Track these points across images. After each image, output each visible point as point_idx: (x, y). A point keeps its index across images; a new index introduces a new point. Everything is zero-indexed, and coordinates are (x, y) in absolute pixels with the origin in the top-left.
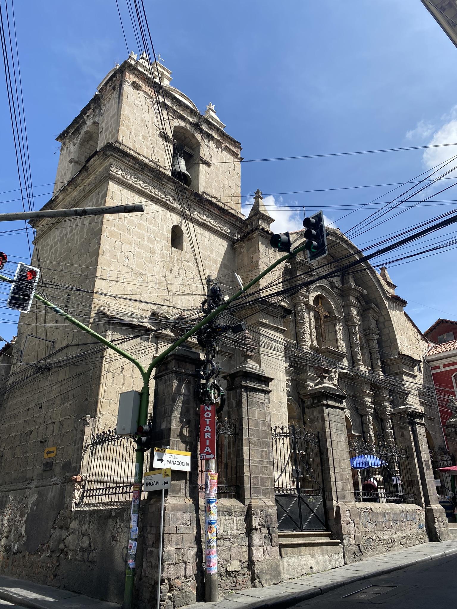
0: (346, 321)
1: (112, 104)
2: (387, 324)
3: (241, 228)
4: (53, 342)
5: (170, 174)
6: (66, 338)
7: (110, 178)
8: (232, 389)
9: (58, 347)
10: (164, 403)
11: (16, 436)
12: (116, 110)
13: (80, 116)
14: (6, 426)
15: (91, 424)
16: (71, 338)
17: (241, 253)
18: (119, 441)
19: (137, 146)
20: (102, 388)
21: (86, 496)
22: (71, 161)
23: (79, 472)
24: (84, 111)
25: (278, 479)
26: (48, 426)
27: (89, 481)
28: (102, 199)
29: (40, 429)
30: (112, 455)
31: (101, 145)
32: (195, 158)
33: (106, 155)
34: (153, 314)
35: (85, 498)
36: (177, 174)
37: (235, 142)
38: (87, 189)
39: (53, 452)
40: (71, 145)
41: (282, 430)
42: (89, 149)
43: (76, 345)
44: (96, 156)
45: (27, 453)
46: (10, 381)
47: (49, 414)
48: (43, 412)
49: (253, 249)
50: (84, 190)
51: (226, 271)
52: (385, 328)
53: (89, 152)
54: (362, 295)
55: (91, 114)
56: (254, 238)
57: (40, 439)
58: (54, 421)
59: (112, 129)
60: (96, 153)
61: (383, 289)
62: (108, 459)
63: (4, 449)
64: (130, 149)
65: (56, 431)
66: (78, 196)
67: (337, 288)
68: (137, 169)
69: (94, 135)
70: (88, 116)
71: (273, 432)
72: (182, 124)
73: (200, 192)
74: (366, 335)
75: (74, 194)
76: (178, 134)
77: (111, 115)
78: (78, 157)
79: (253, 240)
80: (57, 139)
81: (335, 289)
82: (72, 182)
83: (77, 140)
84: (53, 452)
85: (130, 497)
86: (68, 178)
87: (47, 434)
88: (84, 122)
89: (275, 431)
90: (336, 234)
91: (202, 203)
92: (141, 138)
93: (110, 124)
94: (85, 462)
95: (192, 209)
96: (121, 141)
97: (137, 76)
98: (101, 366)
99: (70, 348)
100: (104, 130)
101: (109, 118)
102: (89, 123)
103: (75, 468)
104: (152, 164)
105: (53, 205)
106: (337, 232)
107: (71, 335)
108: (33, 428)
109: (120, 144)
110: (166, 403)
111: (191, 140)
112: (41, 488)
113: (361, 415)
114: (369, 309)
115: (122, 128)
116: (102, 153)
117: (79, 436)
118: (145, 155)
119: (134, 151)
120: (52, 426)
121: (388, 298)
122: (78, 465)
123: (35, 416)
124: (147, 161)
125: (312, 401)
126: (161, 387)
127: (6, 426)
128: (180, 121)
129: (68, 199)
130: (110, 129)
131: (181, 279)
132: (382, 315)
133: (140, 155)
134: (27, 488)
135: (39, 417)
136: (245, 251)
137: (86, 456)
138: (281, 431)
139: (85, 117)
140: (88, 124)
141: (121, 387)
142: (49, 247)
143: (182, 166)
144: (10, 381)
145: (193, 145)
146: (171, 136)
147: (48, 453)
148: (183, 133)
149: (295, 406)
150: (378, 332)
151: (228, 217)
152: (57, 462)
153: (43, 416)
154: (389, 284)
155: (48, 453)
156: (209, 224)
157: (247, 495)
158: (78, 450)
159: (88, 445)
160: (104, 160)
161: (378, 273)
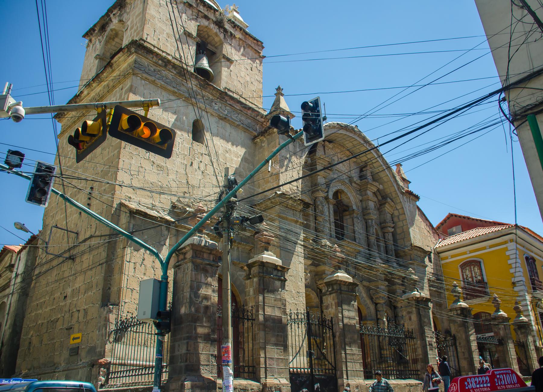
0: (364, 215)
1: (138, 4)
2: (401, 217)
3: (262, 123)
5: (192, 70)
6: (90, 229)
8: (250, 278)
9: (81, 238)
10: (183, 291)
11: (43, 323)
12: (141, 10)
13: (107, 15)
14: (33, 314)
15: (114, 311)
16: (94, 230)
17: (261, 147)
18: (141, 327)
19: (161, 44)
20: (125, 278)
21: (111, 378)
23: (103, 356)
24: (110, 11)
25: (292, 360)
27: (113, 364)
28: (125, 94)
29: (66, 317)
30: (134, 340)
31: (126, 42)
32: (218, 55)
33: (130, 52)
34: (174, 207)
35: (110, 380)
36: (201, 71)
37: (257, 41)
38: (111, 84)
39: (78, 338)
40: (98, 42)
41: (298, 316)
42: (114, 46)
43: (98, 236)
44: (121, 53)
45: (53, 339)
46: (37, 272)
47: (75, 302)
48: (69, 301)
49: (273, 143)
50: (108, 85)
51: (247, 165)
52: (400, 221)
53: (115, 48)
54: (378, 190)
55: (117, 13)
57: (65, 326)
58: (78, 309)
59: (137, 27)
60: (121, 50)
61: (398, 184)
62: (131, 344)
63: (32, 336)
64: (154, 47)
65: (81, 319)
66: (102, 92)
67: (355, 183)
68: (160, 65)
69: (120, 32)
70: (114, 15)
71: (289, 318)
72: (205, 23)
73: (222, 89)
74: (382, 228)
75: (98, 89)
76: (201, 32)
77: (136, 14)
78: (104, 54)
79: (273, 135)
80: (84, 36)
81: (354, 184)
82: (97, 77)
83: (103, 37)
85: (152, 378)
86: (93, 74)
87: (72, 322)
88: (111, 20)
89: (291, 317)
90: (354, 131)
91: (224, 98)
92: (165, 35)
93: (135, 22)
94: (108, 347)
95: (214, 104)
96: (145, 39)
98: (123, 257)
99: (93, 239)
100: (129, 28)
101: (135, 17)
102: (115, 21)
103: (100, 352)
104: (176, 61)
105: (78, 100)
106: (355, 129)
107: (94, 226)
108: (59, 316)
109: (145, 41)
110: (185, 291)
111: (214, 39)
113: (375, 303)
114: (385, 203)
115: (147, 27)
116: (126, 50)
117: (103, 323)
118: (168, 52)
119: (158, 49)
120: (77, 313)
121: (402, 193)
122: (102, 349)
123: (61, 304)
124: (170, 58)
125: (326, 289)
126: (180, 275)
127: (33, 314)
129: (93, 94)
130: (135, 28)
131: (201, 173)
132: (397, 209)
133: (163, 52)
135: (65, 305)
136: (266, 145)
138: (296, 317)
139: (112, 16)
140: (114, 23)
141: (142, 277)
143: (205, 63)
144: (37, 272)
145: (216, 43)
146: (195, 34)
147: (74, 339)
148: (206, 31)
149: (313, 295)
150: (393, 225)
152: (82, 347)
153: (68, 304)
154: (404, 180)
155: (74, 339)
156: (230, 118)
157: (262, 375)
158: (102, 336)
159: (112, 332)
160: (128, 57)
161: (394, 168)
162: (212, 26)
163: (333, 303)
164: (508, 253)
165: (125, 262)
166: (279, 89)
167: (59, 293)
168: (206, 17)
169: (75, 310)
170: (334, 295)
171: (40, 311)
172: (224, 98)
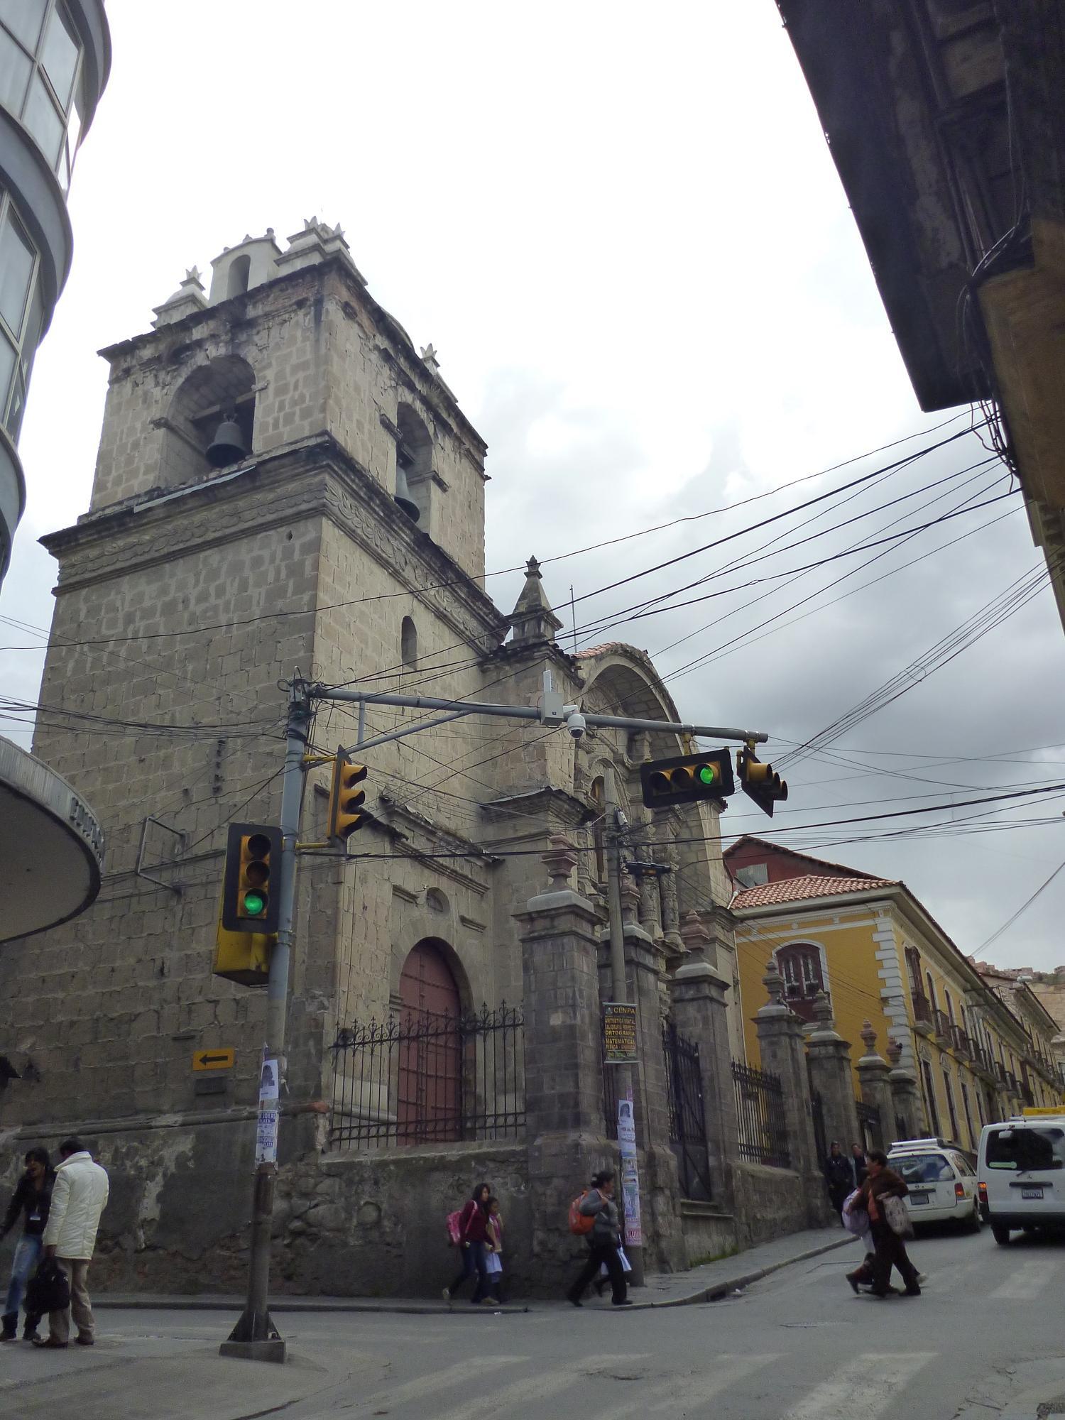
4: (182, 836)
7: (324, 514)
11: (72, 1024)
14: (30, 999)
22: (158, 424)
26: (193, 1007)
39: (225, 1058)
48: (172, 980)
56: (534, 659)
58: (214, 998)
72: (408, 397)
84: (225, 1058)
91: (444, 573)
92: (354, 425)
97: (348, 288)
108: (141, 1009)
110: (559, 984)
112: (203, 1127)
128: (406, 392)
132: (688, 827)
134: (151, 1128)
137: (326, 1067)
142: (121, 615)
147: (205, 1060)
151: (479, 604)
162: (418, 406)
163: (699, 1017)
164: (876, 937)
165: (342, 912)
166: (533, 564)
167: (132, 961)
168: (412, 387)
169: (199, 999)
170: (701, 1002)
171: (61, 995)
172: (444, 573)
